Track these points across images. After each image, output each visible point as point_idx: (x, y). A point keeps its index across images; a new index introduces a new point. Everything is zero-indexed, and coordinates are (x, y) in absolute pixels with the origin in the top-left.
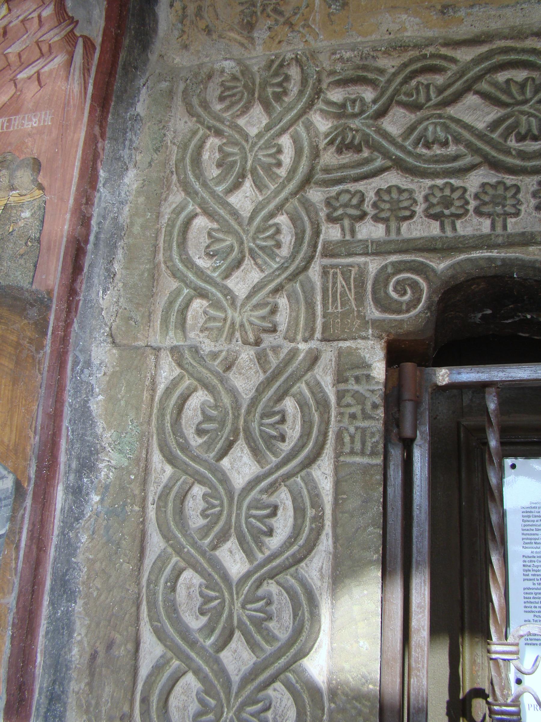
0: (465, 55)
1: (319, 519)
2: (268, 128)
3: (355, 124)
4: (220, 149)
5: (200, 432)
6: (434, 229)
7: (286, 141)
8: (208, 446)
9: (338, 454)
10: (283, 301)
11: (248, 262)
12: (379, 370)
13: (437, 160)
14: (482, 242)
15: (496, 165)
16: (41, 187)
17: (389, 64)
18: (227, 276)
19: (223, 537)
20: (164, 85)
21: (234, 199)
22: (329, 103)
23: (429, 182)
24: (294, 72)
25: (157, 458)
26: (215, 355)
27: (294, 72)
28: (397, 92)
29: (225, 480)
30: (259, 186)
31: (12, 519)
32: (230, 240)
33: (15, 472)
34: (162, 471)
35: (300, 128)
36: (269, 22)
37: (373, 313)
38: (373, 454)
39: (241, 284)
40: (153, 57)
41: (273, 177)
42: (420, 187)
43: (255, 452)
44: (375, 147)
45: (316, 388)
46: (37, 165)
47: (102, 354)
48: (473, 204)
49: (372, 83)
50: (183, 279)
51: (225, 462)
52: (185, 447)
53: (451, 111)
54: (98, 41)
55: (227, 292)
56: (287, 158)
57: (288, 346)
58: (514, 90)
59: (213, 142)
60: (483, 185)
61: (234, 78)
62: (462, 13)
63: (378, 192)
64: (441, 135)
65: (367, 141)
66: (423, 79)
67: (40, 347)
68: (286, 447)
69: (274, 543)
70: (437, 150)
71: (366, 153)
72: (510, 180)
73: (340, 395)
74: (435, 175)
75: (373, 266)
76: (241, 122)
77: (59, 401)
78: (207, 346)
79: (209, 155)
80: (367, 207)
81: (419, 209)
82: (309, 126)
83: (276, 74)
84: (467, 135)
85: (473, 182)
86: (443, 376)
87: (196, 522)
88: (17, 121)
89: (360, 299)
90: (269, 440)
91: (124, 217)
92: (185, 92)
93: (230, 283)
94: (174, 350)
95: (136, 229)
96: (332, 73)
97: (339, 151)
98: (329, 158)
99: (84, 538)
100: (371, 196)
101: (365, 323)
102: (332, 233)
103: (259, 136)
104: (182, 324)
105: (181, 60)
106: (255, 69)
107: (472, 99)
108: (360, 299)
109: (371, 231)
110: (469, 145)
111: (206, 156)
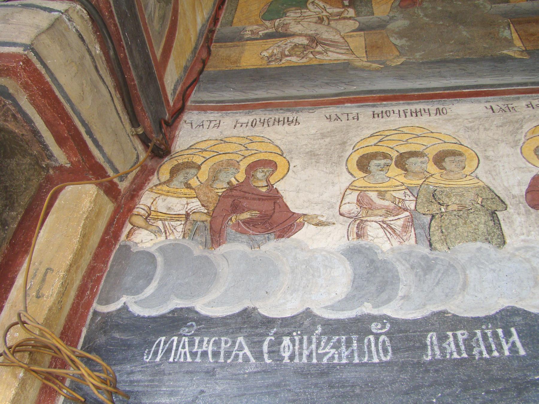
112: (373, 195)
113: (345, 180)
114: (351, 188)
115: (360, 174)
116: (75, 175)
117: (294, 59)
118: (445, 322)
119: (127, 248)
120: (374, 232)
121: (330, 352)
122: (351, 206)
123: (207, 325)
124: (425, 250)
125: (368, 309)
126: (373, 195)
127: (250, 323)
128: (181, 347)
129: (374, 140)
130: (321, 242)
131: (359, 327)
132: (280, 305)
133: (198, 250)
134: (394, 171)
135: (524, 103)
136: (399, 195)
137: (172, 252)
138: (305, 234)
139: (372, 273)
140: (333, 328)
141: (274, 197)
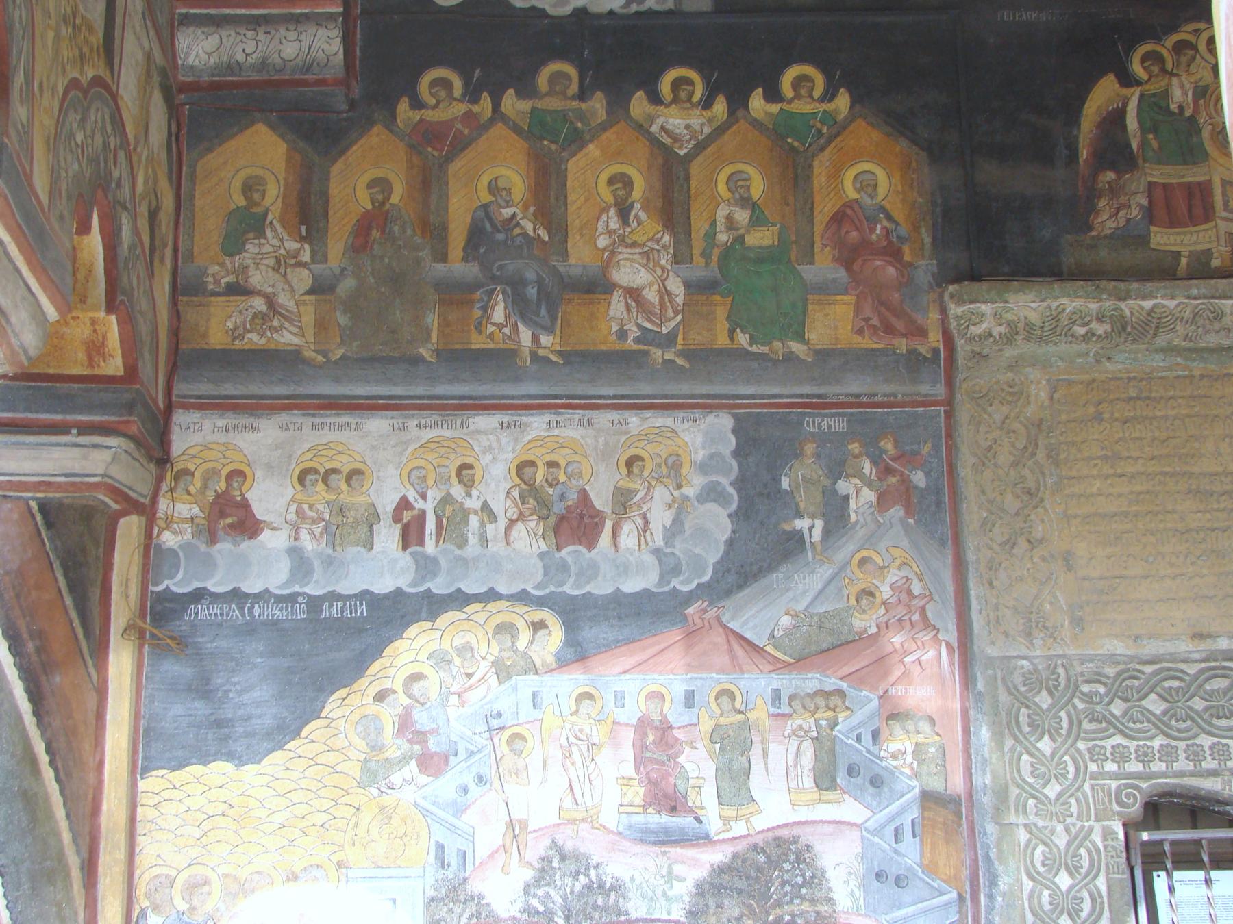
0: (1148, 669)
1: (1102, 903)
2: (1052, 706)
3: (1098, 708)
4: (1029, 716)
5: (1044, 865)
6: (1140, 767)
7: (1063, 714)
8: (1049, 871)
9: (1108, 874)
10: (1073, 801)
11: (1053, 780)
12: (1121, 836)
13: (1140, 731)
14: (1163, 775)
15: (1167, 735)
16: (938, 734)
17: (1111, 671)
18: (1044, 785)
19: (1061, 913)
20: (991, 672)
21: (1038, 745)
22: (1082, 693)
23: (1136, 743)
24: (1061, 671)
25: (1025, 878)
26: (1046, 828)
27: (1061, 671)
28: (1117, 691)
29: (1058, 888)
30: (1053, 739)
31: (960, 912)
32: (1043, 769)
33: (957, 889)
34: (1028, 884)
35: (1070, 707)
36: (1042, 635)
37: (1116, 808)
38: (1123, 873)
39: (1052, 790)
40: (976, 648)
41: (1060, 735)
42: (1132, 745)
43: (1071, 874)
44: (1109, 722)
45: (1094, 844)
46: (932, 721)
47: (990, 828)
48: (1157, 755)
49: (1105, 684)
50: (1023, 789)
51: (1057, 880)
52: (1038, 873)
53: (1143, 702)
54: (955, 645)
55: (1046, 797)
56: (1065, 724)
57: (1079, 824)
58: (1174, 693)
59: (1023, 710)
60: (1161, 745)
61: (1031, 673)
62: (1145, 642)
63: (1113, 747)
64: (1140, 717)
65: (1105, 719)
66: (1127, 683)
67: (960, 825)
68: (1083, 871)
69: (1084, 915)
70: (1139, 725)
71: (1104, 724)
72: (1173, 743)
73: (1105, 847)
74: (1140, 740)
75: (1114, 785)
76: (1037, 700)
77: (976, 854)
78: (1041, 824)
79: (1023, 719)
80: (1108, 754)
81: (1133, 756)
82: (1075, 707)
83: (1053, 673)
84: (1153, 718)
85: (1157, 743)
86: (1145, 836)
87: (1047, 907)
88: (911, 690)
89: (1110, 802)
90: (1076, 868)
91: (987, 755)
92: (1003, 679)
93: (1046, 791)
94: (1026, 826)
95: (994, 761)
96: (1082, 675)
97: (1090, 722)
98: (1086, 725)
99: (997, 919)
100: (1109, 749)
101: (1114, 813)
102: (1093, 767)
103: (1049, 709)
104: (1025, 813)
105: (992, 652)
106: (1040, 667)
107: (1153, 696)
108: (1110, 802)
109: (1111, 767)
110: (1154, 724)
111: (1021, 719)
112: (305, 507)
113: (289, 492)
114: (293, 500)
115: (299, 487)
116: (124, 513)
117: (254, 337)
118: (334, 597)
119: (158, 546)
120: (304, 535)
121: (278, 613)
122: (292, 517)
123: (215, 597)
124: (330, 551)
125: (297, 589)
126: (305, 507)
127: (236, 595)
128: (203, 612)
129: (310, 455)
130: (274, 541)
131: (292, 599)
132: (252, 586)
133: (203, 548)
134: (321, 486)
135: (415, 422)
136: (321, 507)
137: (186, 547)
138: (266, 535)
139: (301, 565)
140: (280, 599)
141: (245, 506)
